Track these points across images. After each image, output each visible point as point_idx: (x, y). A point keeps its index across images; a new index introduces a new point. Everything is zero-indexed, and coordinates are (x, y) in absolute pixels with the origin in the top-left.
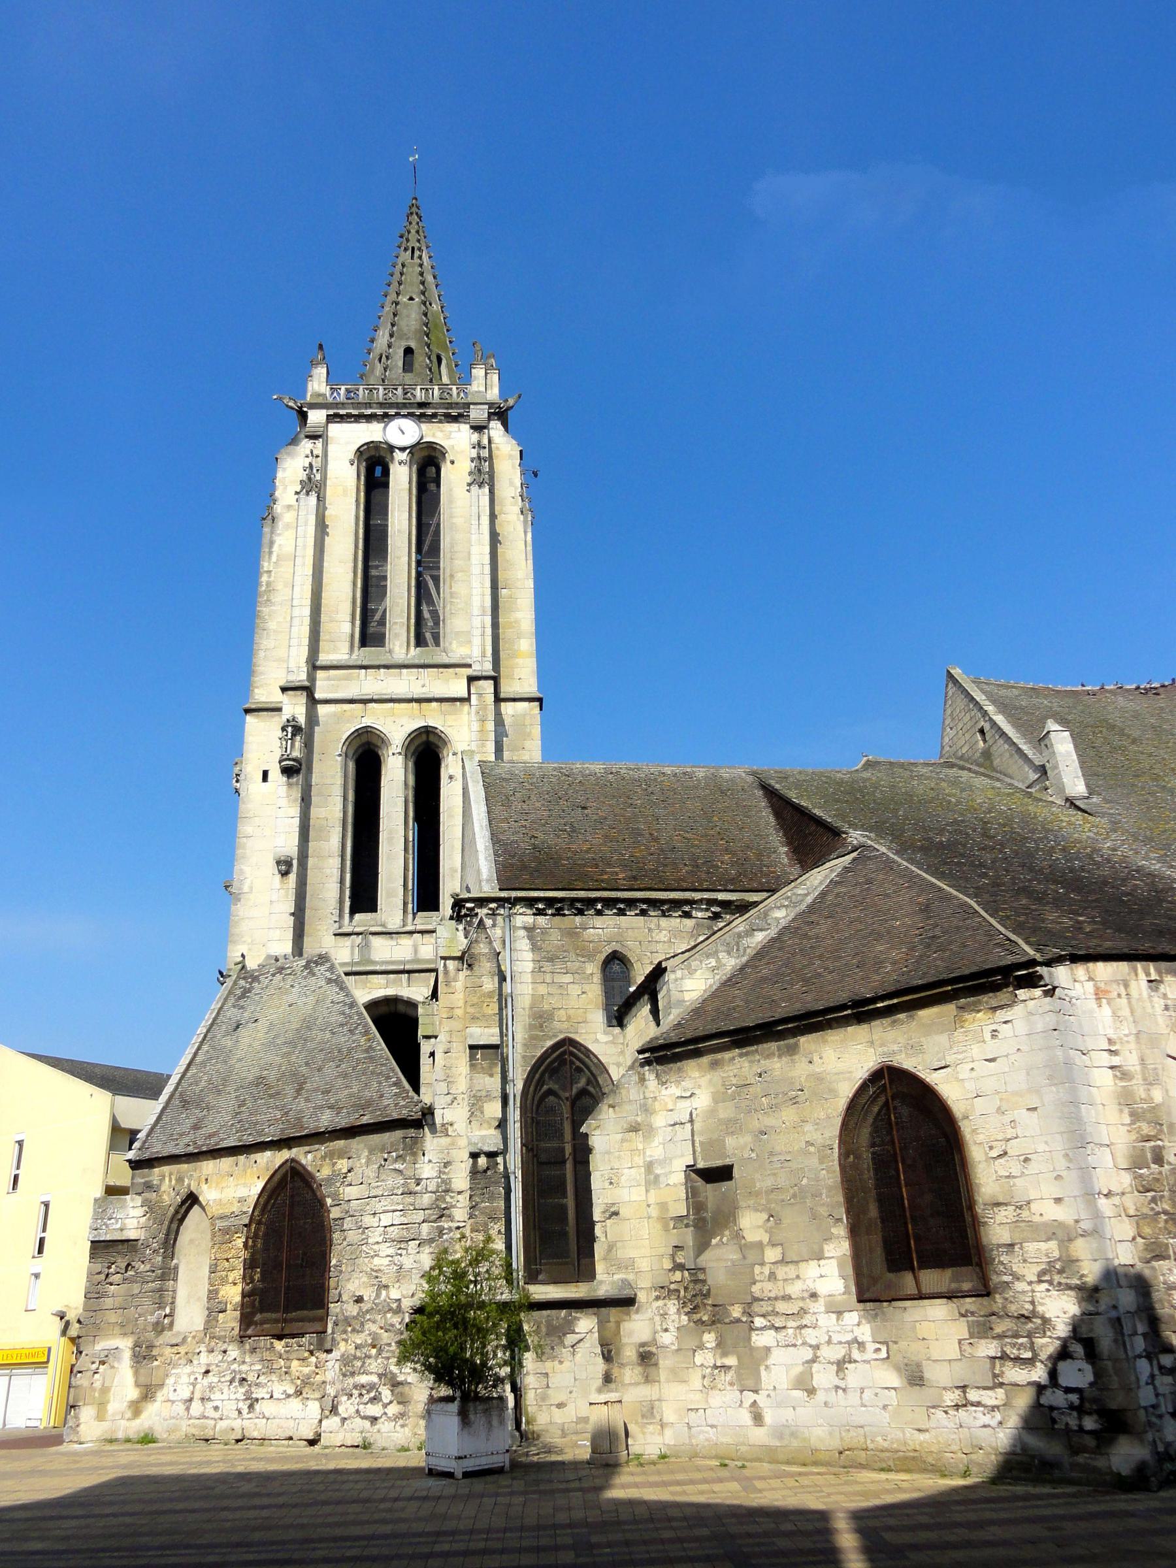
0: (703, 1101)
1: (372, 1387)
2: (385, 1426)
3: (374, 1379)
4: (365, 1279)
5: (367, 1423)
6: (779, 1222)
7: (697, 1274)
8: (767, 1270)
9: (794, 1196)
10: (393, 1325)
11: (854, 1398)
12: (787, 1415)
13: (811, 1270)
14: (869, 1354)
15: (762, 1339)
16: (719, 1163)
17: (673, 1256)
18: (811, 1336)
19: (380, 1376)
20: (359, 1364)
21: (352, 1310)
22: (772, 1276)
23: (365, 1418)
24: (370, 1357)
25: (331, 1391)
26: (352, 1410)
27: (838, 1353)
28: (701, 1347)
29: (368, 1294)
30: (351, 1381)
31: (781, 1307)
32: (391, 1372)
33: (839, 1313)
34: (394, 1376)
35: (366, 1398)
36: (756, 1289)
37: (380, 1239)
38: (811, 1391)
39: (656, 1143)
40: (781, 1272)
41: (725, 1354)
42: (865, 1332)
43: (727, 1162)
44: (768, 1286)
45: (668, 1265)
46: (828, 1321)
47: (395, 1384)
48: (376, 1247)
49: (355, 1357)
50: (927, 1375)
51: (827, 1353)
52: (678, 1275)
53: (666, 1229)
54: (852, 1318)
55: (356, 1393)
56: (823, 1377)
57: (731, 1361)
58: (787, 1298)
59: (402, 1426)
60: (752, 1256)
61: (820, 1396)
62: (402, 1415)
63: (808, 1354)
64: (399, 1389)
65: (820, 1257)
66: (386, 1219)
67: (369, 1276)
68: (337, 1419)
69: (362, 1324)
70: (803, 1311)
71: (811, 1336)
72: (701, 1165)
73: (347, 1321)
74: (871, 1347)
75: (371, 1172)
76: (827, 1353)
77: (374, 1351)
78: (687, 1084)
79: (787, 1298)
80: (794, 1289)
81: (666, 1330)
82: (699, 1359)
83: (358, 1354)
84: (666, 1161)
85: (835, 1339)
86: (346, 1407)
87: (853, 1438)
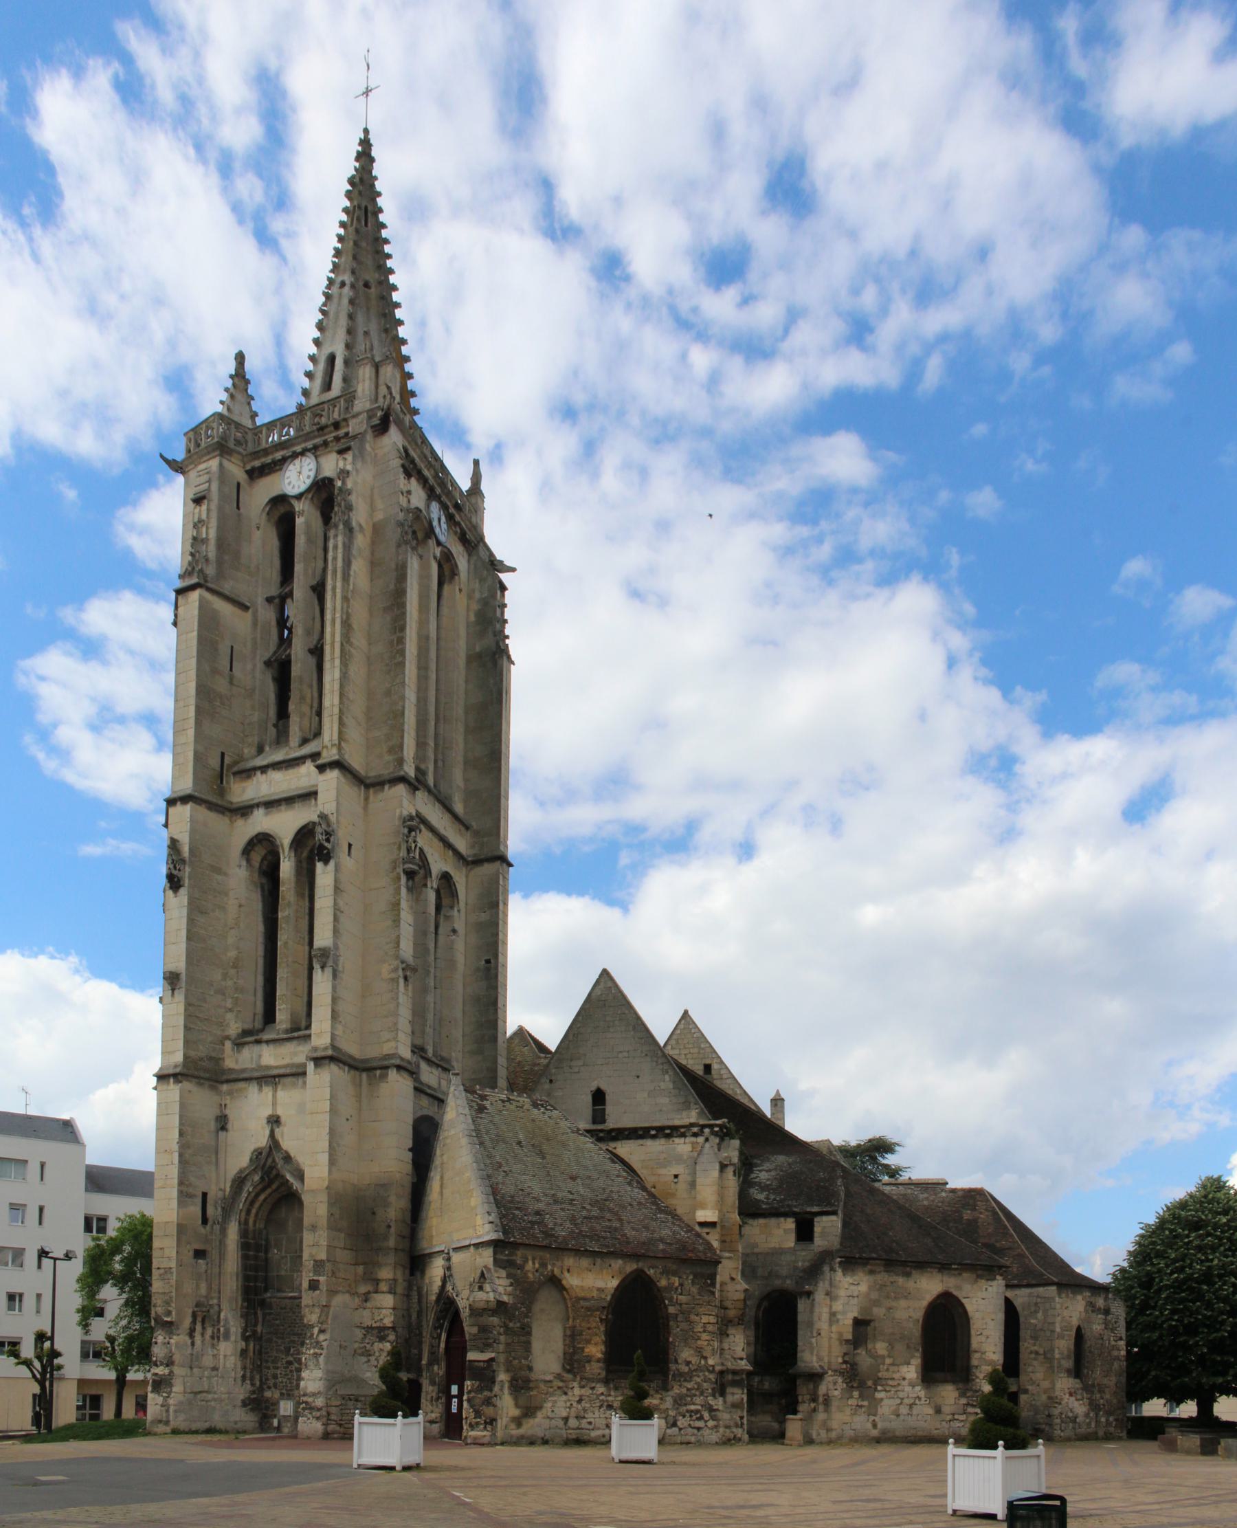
0: (863, 1288)
1: (697, 1411)
2: (706, 1432)
3: (699, 1407)
4: (692, 1352)
5: (695, 1431)
6: (893, 1348)
7: (854, 1366)
8: (885, 1367)
9: (901, 1338)
10: (710, 1379)
11: (914, 1418)
12: (887, 1425)
13: (904, 1369)
14: (922, 1402)
15: (878, 1395)
16: (868, 1318)
17: (843, 1357)
18: (901, 1395)
19: (702, 1406)
20: (689, 1399)
21: (685, 1369)
22: (888, 1370)
23: (694, 1428)
24: (695, 1395)
25: (672, 1413)
26: (686, 1424)
27: (912, 1401)
28: (852, 1397)
29: (694, 1360)
30: (683, 1409)
31: (891, 1383)
32: (709, 1404)
33: (913, 1386)
34: (711, 1406)
35: (694, 1417)
36: (880, 1375)
37: (701, 1330)
38: (898, 1415)
39: (839, 1303)
40: (892, 1369)
41: (863, 1400)
42: (922, 1394)
43: (873, 1318)
44: (885, 1373)
45: (840, 1360)
46: (908, 1389)
47: (711, 1410)
48: (699, 1334)
49: (687, 1396)
50: (943, 1410)
51: (906, 1401)
52: (844, 1366)
53: (841, 1344)
54: (918, 1388)
55: (688, 1415)
56: (904, 1410)
57: (865, 1403)
58: (893, 1379)
59: (716, 1432)
60: (880, 1361)
61: (902, 1417)
62: (716, 1427)
63: (898, 1401)
64: (713, 1413)
65: (909, 1364)
66: (705, 1319)
67: (696, 1351)
68: (675, 1430)
69: (691, 1377)
70: (899, 1384)
71: (901, 1395)
72: (860, 1317)
73: (681, 1374)
74: (923, 1399)
75: (694, 1290)
76: (906, 1401)
77: (698, 1393)
78: (855, 1278)
79: (893, 1379)
80: (896, 1376)
81: (836, 1389)
82: (850, 1403)
83: (689, 1393)
84: (844, 1313)
85: (910, 1396)
86: (682, 1422)
87: (913, 1432)
